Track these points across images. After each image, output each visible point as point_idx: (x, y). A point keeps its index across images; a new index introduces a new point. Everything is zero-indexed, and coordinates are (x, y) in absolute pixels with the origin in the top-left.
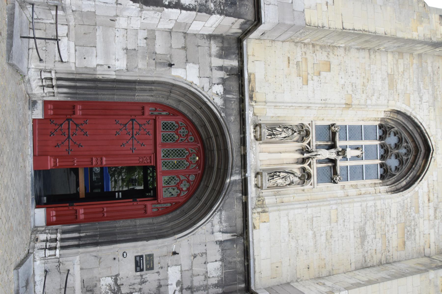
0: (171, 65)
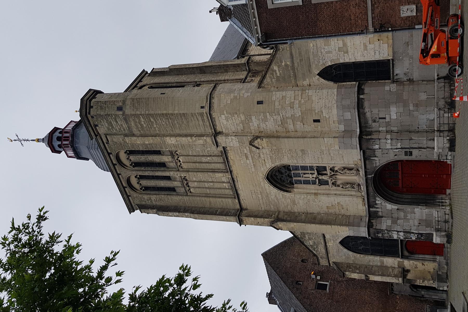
0: (398, 209)
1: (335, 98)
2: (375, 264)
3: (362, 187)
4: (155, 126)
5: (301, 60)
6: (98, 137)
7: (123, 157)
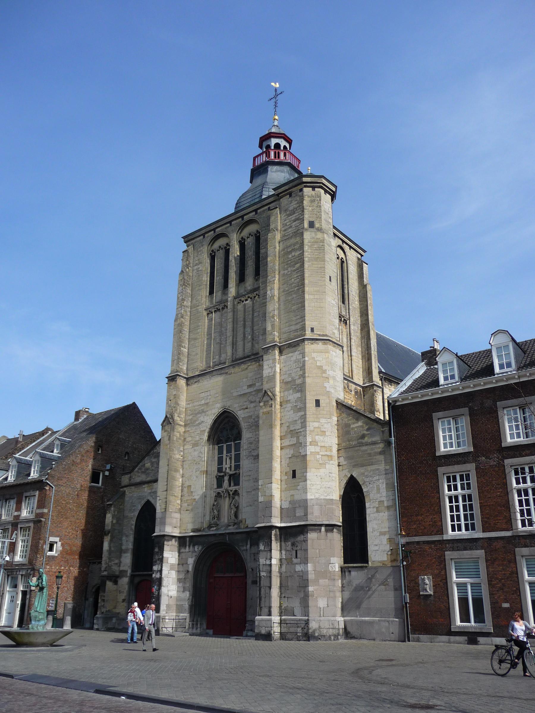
0: (188, 571)
1: (322, 497)
2: (124, 542)
3: (215, 528)
4: (289, 269)
5: (370, 455)
6: (276, 197)
7: (252, 228)
